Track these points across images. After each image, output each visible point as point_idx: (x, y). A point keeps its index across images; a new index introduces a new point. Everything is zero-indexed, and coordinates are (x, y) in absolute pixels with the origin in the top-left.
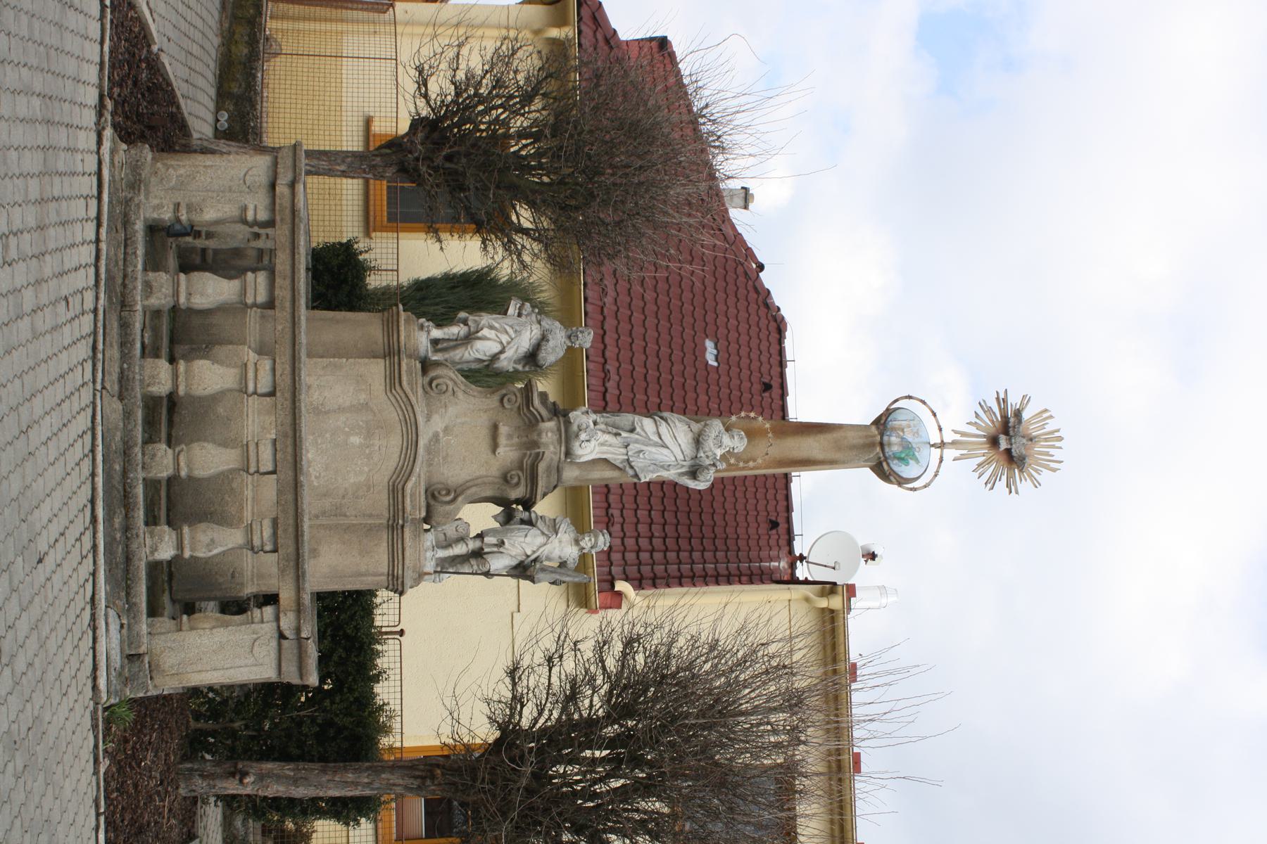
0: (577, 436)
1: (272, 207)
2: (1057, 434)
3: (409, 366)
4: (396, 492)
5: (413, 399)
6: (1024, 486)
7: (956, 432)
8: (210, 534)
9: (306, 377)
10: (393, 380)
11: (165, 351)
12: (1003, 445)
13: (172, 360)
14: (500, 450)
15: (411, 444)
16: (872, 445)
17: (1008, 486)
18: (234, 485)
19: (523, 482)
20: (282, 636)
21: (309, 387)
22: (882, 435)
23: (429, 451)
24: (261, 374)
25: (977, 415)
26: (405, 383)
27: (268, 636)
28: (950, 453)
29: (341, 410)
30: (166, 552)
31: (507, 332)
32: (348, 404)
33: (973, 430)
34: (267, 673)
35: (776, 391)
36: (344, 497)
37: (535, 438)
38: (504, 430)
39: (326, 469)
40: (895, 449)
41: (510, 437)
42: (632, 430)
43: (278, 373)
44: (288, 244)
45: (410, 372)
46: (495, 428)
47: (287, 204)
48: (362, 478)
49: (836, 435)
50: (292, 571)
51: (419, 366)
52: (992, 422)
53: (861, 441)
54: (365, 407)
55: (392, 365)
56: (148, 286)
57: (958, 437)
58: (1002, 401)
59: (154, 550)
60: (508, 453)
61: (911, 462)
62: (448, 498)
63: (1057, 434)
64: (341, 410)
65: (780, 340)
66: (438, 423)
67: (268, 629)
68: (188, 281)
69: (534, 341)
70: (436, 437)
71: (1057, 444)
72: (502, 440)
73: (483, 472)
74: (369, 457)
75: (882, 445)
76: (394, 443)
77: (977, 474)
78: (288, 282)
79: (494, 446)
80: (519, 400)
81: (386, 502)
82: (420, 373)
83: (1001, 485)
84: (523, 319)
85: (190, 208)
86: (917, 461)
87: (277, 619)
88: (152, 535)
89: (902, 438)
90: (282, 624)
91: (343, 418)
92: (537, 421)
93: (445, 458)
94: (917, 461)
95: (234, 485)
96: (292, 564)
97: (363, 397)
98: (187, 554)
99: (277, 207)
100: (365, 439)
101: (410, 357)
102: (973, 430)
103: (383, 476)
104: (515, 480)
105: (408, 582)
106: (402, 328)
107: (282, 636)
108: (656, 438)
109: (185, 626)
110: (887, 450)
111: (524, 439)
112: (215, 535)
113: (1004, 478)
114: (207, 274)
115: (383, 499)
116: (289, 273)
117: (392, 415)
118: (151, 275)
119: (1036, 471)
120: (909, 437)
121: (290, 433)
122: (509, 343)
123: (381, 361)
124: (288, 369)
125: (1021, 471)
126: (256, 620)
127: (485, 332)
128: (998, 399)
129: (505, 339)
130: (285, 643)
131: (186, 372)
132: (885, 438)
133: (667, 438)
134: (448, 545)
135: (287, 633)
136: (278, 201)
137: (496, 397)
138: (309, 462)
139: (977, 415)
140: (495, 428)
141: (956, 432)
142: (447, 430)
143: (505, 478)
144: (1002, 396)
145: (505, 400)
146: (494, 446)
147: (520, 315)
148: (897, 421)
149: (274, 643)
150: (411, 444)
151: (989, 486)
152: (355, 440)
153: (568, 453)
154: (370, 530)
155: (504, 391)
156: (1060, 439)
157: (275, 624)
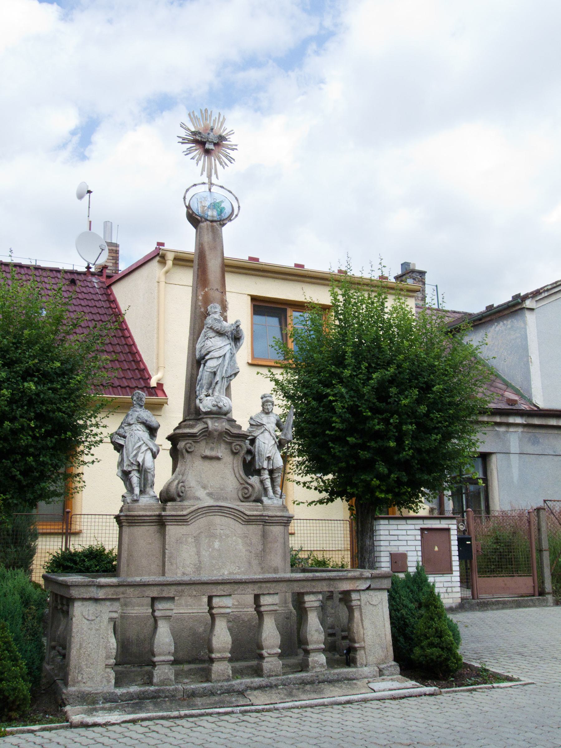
0: (220, 408)
1: (534, 591)
2: (203, 112)
3: (171, 509)
4: (249, 520)
5: (193, 509)
6: (232, 140)
7: (202, 174)
8: (313, 632)
9: (178, 577)
10: (182, 520)
11: (205, 665)
12: (211, 147)
13: (212, 661)
14: (220, 455)
15: (220, 510)
16: (212, 226)
17: (233, 149)
18: (246, 619)
19: (239, 443)
20: (368, 588)
21: (184, 574)
22: (207, 220)
23: (217, 499)
24: (221, 604)
25: (193, 158)
26: (185, 513)
27: (367, 596)
28: (214, 180)
29: (198, 553)
30: (322, 658)
31: (140, 446)
32: (195, 549)
33: (201, 163)
34: (384, 596)
35: (76, 277)
36: (251, 552)
37: (217, 433)
38: (208, 453)
39: (235, 563)
40: (215, 213)
41: (212, 449)
42: (215, 374)
43: (223, 593)
44: (160, 587)
45: (174, 509)
46: (205, 458)
47: (113, 590)
48: (240, 541)
49: (206, 247)
50: (336, 582)
51: (169, 504)
52: (196, 150)
53: (210, 233)
54: (197, 539)
55: (171, 521)
56: (162, 683)
57: (205, 173)
58: (184, 141)
59: (322, 665)
60: (221, 451)
61: (223, 205)
62: (250, 488)
63: (203, 112)
64: (198, 553)
65: (44, 269)
66: (201, 493)
67: (364, 596)
68: (160, 654)
69: (144, 429)
70: (210, 495)
71: (209, 112)
72: (213, 454)
73: (230, 466)
74: (227, 536)
75: (212, 221)
76: (218, 520)
77: (226, 167)
78: (165, 588)
79: (218, 459)
80: (190, 441)
81: (254, 526)
82: (174, 503)
83: (232, 154)
84: (127, 435)
85: (108, 657)
86: (222, 202)
87: (359, 591)
88: (313, 667)
89: (209, 208)
90: (363, 588)
91: (204, 553)
92: (207, 431)
93: (222, 490)
94: (222, 202)
95: (246, 619)
96: (332, 583)
97: (190, 540)
98: (323, 646)
99: (115, 597)
100: (216, 538)
101: (164, 509)
102: (201, 163)
103: (239, 528)
104: (238, 447)
105: (285, 514)
106: (136, 513)
107: (368, 588)
108: (221, 359)
109: (362, 644)
110: (215, 219)
111: (216, 440)
112: (313, 629)
113: (228, 151)
114: (156, 641)
115: (252, 528)
116: (159, 588)
117: (202, 522)
118: (155, 680)
119: (224, 131)
120: (207, 204)
121: (259, 584)
122: (147, 445)
123: (168, 528)
124: (221, 587)
125: (226, 140)
126: (359, 603)
127: (140, 460)
128: (182, 143)
129: (144, 448)
130: (372, 587)
131: (219, 652)
132: (209, 218)
133: (221, 353)
134: (265, 490)
135: (367, 586)
136: (110, 597)
137: (186, 455)
138: (230, 573)
139: (193, 158)
140: (205, 458)
141: (202, 174)
142: (204, 487)
143: (234, 454)
144: (181, 140)
145: (190, 450)
146: (218, 459)
147: (125, 437)
148: (196, 207)
149: (371, 593)
150: (220, 510)
151: (232, 161)
152: (217, 544)
153: (225, 414)
154: (264, 535)
155: (184, 451)
156: (206, 110)
157: (361, 592)
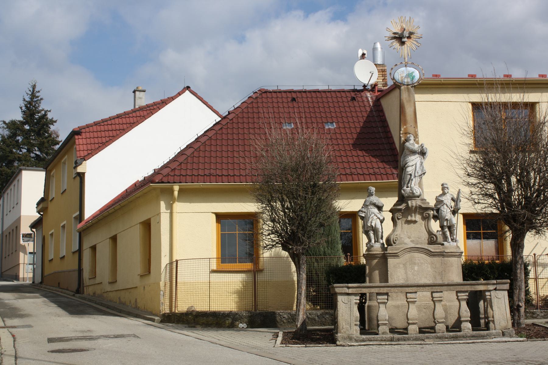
10: (395, 255)
16: (408, 88)
22: (404, 85)
24: (412, 297)
30: (469, 325)
39: (426, 278)
40: (409, 80)
45: (392, 250)
53: (407, 92)
54: (405, 265)
56: (383, 333)
59: (469, 329)
61: (414, 74)
64: (406, 273)
66: (407, 241)
67: (493, 293)
68: (381, 321)
70: (412, 241)
72: (413, 219)
74: (422, 263)
75: (408, 85)
79: (415, 222)
86: (413, 72)
88: (464, 330)
89: (405, 77)
91: (409, 272)
94: (413, 72)
97: (401, 266)
98: (469, 319)
108: (414, 167)
120: (405, 75)
130: (498, 288)
142: (409, 238)
146: (415, 222)
149: (497, 292)
152: (416, 268)
153: (418, 197)
